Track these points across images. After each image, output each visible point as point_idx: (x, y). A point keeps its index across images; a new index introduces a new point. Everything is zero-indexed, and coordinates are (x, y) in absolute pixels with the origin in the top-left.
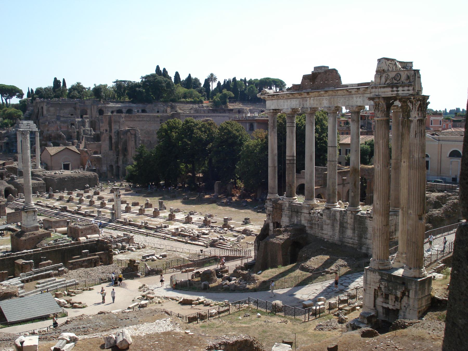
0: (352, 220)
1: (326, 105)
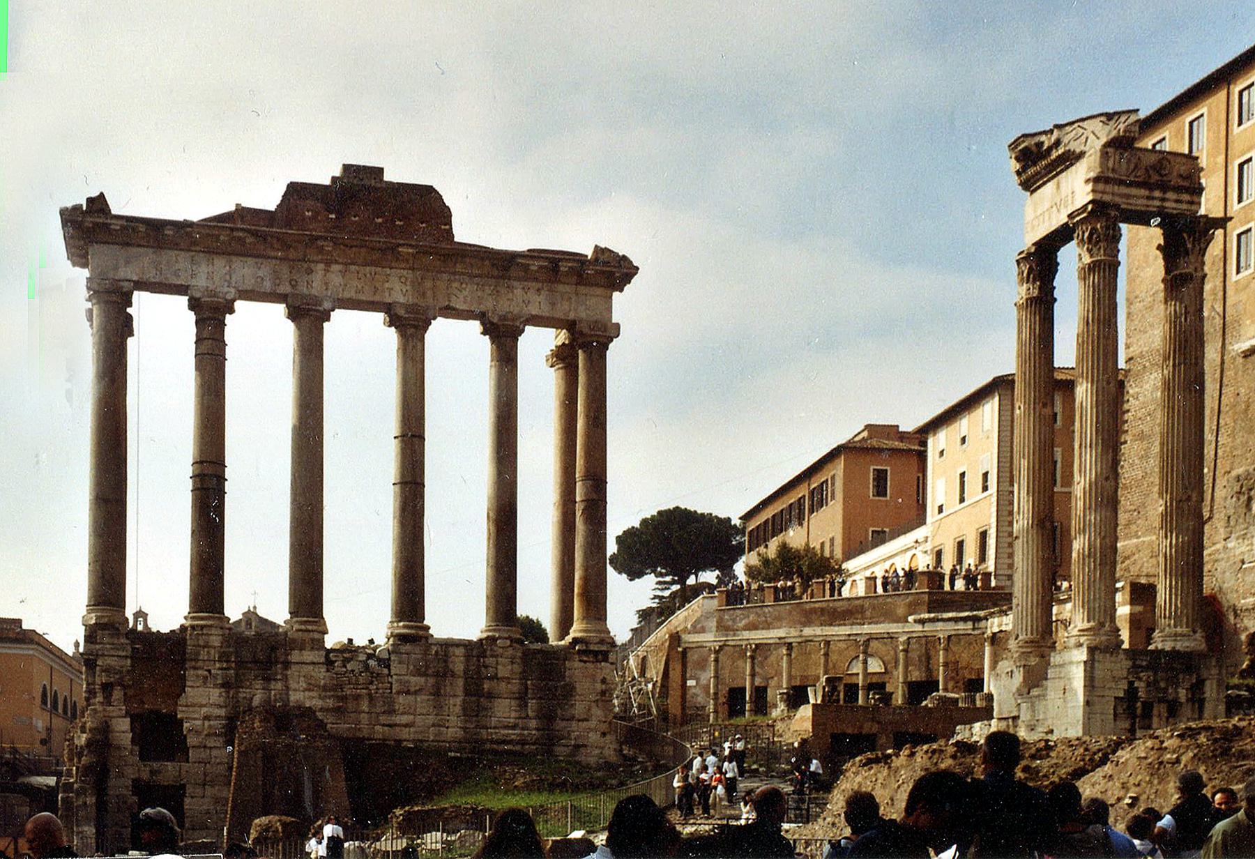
1: (402, 300)
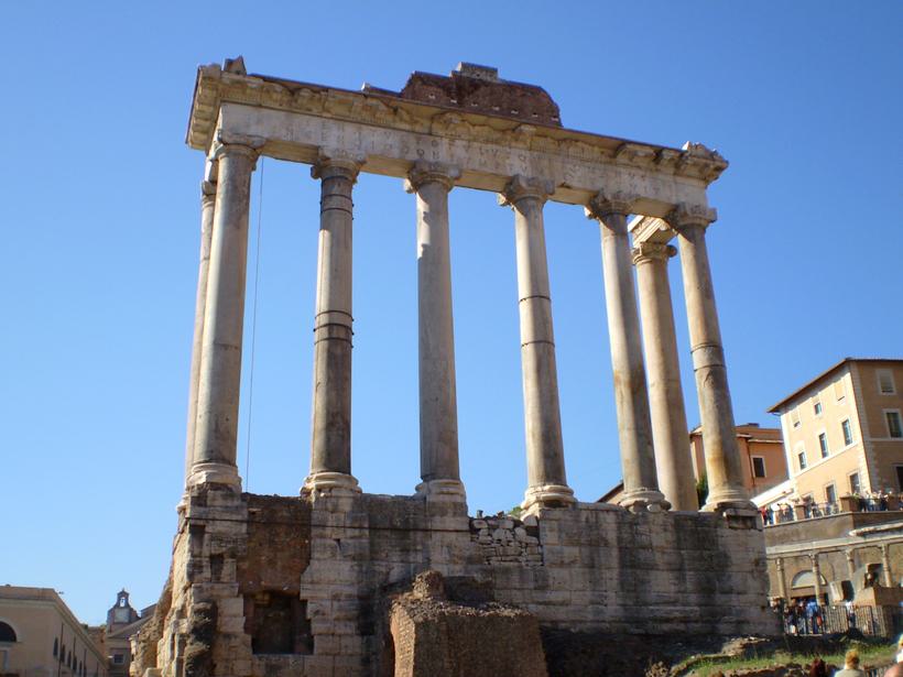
0: (670, 536)
